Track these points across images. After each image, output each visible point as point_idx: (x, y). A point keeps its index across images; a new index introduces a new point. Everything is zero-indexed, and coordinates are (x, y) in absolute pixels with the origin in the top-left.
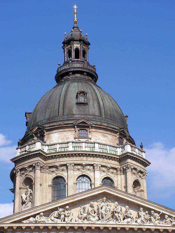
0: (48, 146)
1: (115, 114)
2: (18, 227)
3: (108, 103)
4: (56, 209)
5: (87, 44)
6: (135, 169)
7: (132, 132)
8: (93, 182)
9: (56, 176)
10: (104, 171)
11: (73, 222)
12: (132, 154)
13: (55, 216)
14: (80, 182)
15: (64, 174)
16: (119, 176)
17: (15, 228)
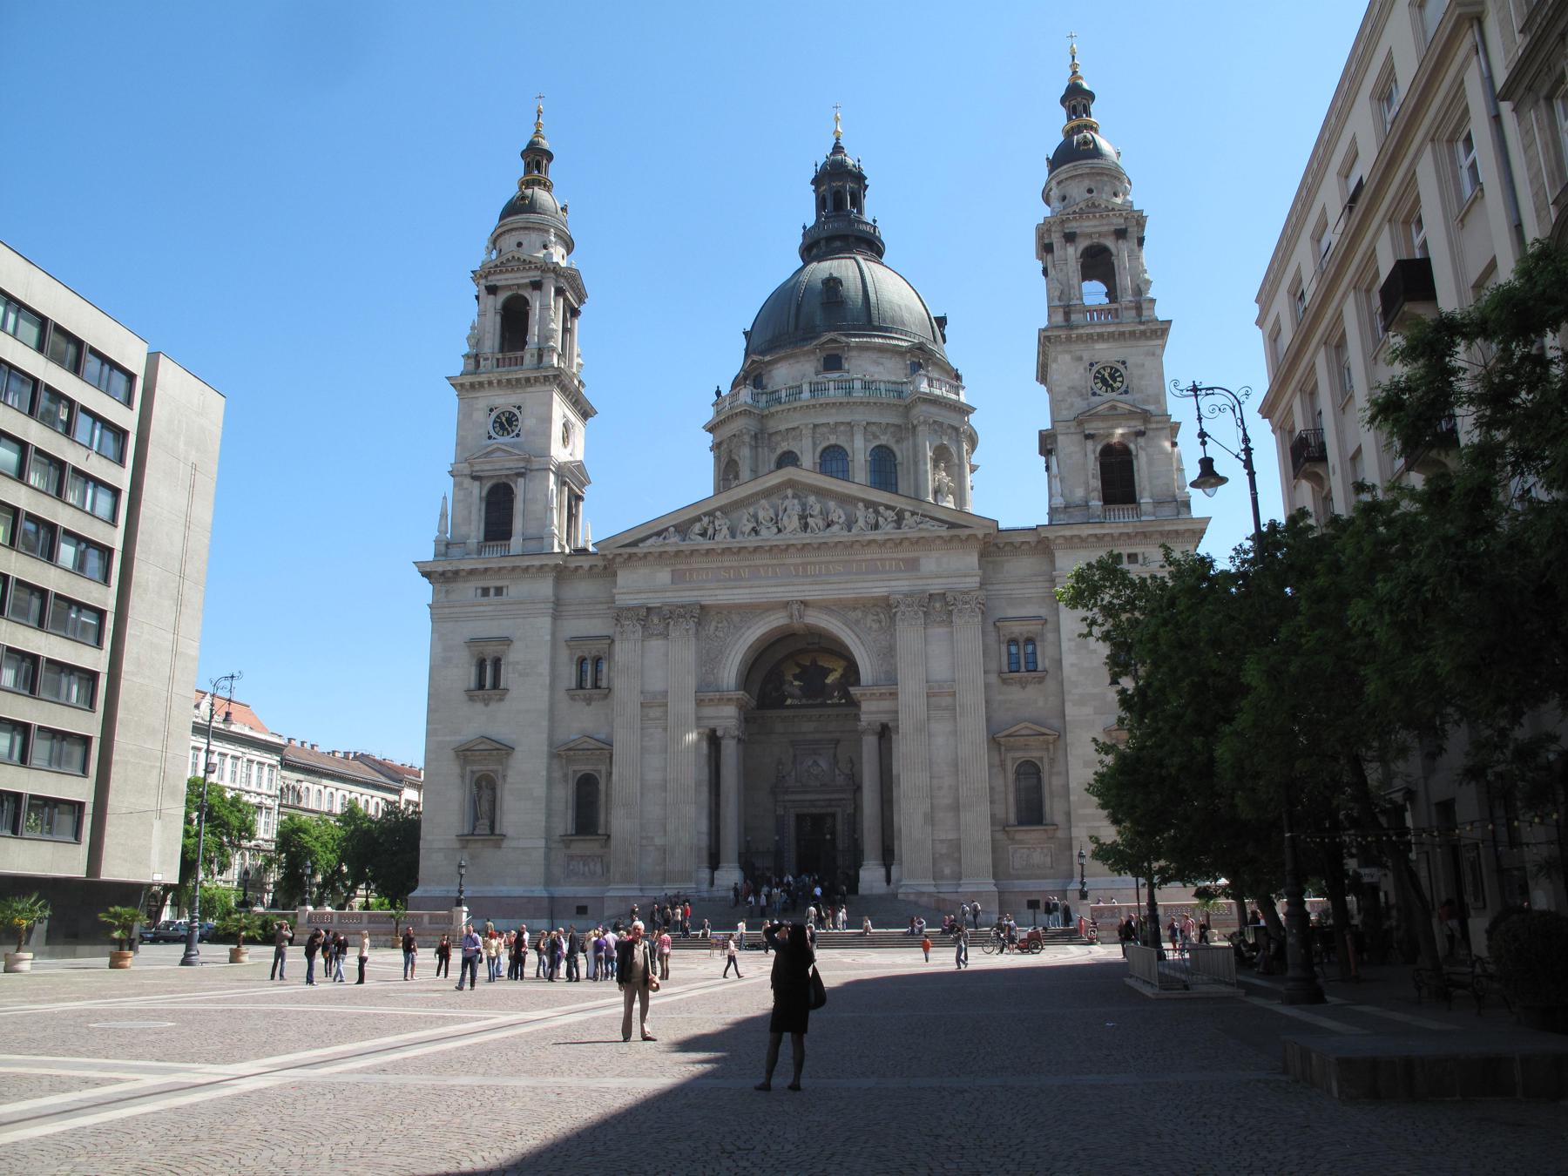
0: (766, 393)
1: (906, 316)
2: (630, 556)
4: (698, 519)
5: (859, 178)
6: (935, 422)
7: (953, 352)
12: (930, 394)
14: (828, 458)
17: (626, 556)
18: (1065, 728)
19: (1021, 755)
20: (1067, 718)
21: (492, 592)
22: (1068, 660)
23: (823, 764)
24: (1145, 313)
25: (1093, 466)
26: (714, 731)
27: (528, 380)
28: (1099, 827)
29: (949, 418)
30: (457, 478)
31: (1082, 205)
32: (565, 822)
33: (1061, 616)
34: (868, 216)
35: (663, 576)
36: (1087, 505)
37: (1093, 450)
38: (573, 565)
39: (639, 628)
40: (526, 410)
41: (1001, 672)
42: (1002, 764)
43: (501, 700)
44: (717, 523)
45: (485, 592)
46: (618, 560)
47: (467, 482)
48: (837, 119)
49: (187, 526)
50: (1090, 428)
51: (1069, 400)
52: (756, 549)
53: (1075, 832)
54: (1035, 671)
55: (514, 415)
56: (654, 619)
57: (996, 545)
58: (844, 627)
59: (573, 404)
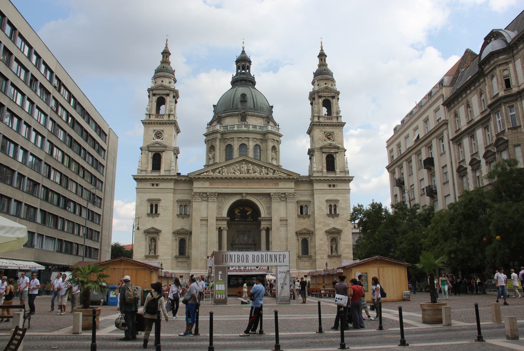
0: (223, 126)
1: (264, 106)
2: (198, 178)
3: (259, 100)
5: (250, 62)
7: (276, 115)
8: (248, 147)
9: (227, 144)
10: (255, 141)
11: (227, 175)
13: (218, 172)
15: (232, 143)
16: (263, 144)
18: (315, 230)
19: (303, 237)
20: (316, 228)
21: (155, 185)
22: (316, 212)
23: (246, 238)
24: (339, 119)
25: (324, 161)
26: (220, 228)
27: (166, 123)
28: (323, 256)
29: (276, 138)
30: (143, 151)
31: (324, 88)
32: (176, 252)
33: (315, 200)
34: (252, 73)
35: (207, 184)
36: (322, 172)
37: (325, 156)
38: (179, 179)
39: (200, 198)
40: (165, 132)
41: (298, 216)
42: (298, 240)
43: (158, 217)
44: (223, 170)
45: (153, 185)
46: (194, 179)
47: (147, 152)
48: (243, 43)
49: (113, 175)
50: (324, 150)
51: (319, 142)
52: (235, 178)
53: (317, 257)
54: (307, 214)
55: (161, 133)
56: (205, 196)
57: (298, 180)
58: (258, 201)
59: (176, 130)
